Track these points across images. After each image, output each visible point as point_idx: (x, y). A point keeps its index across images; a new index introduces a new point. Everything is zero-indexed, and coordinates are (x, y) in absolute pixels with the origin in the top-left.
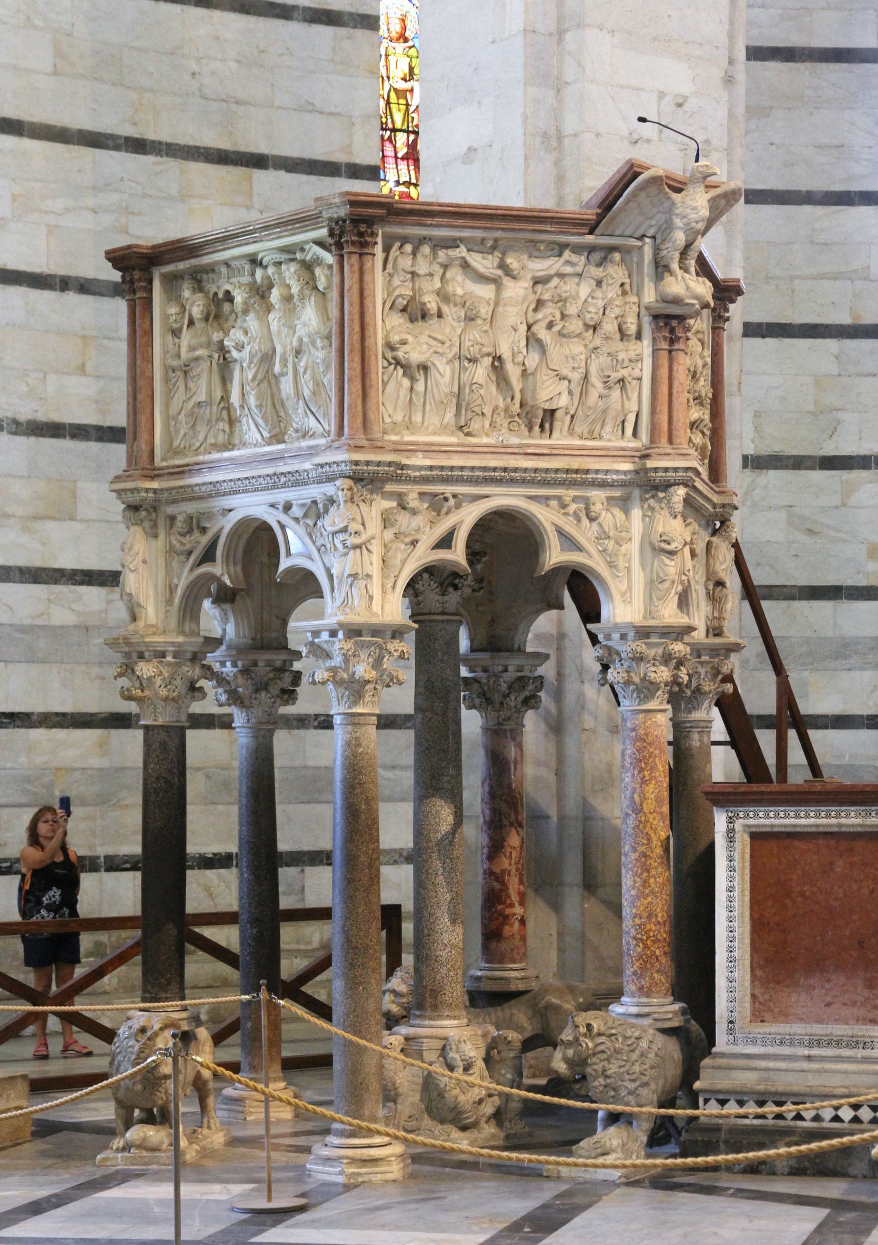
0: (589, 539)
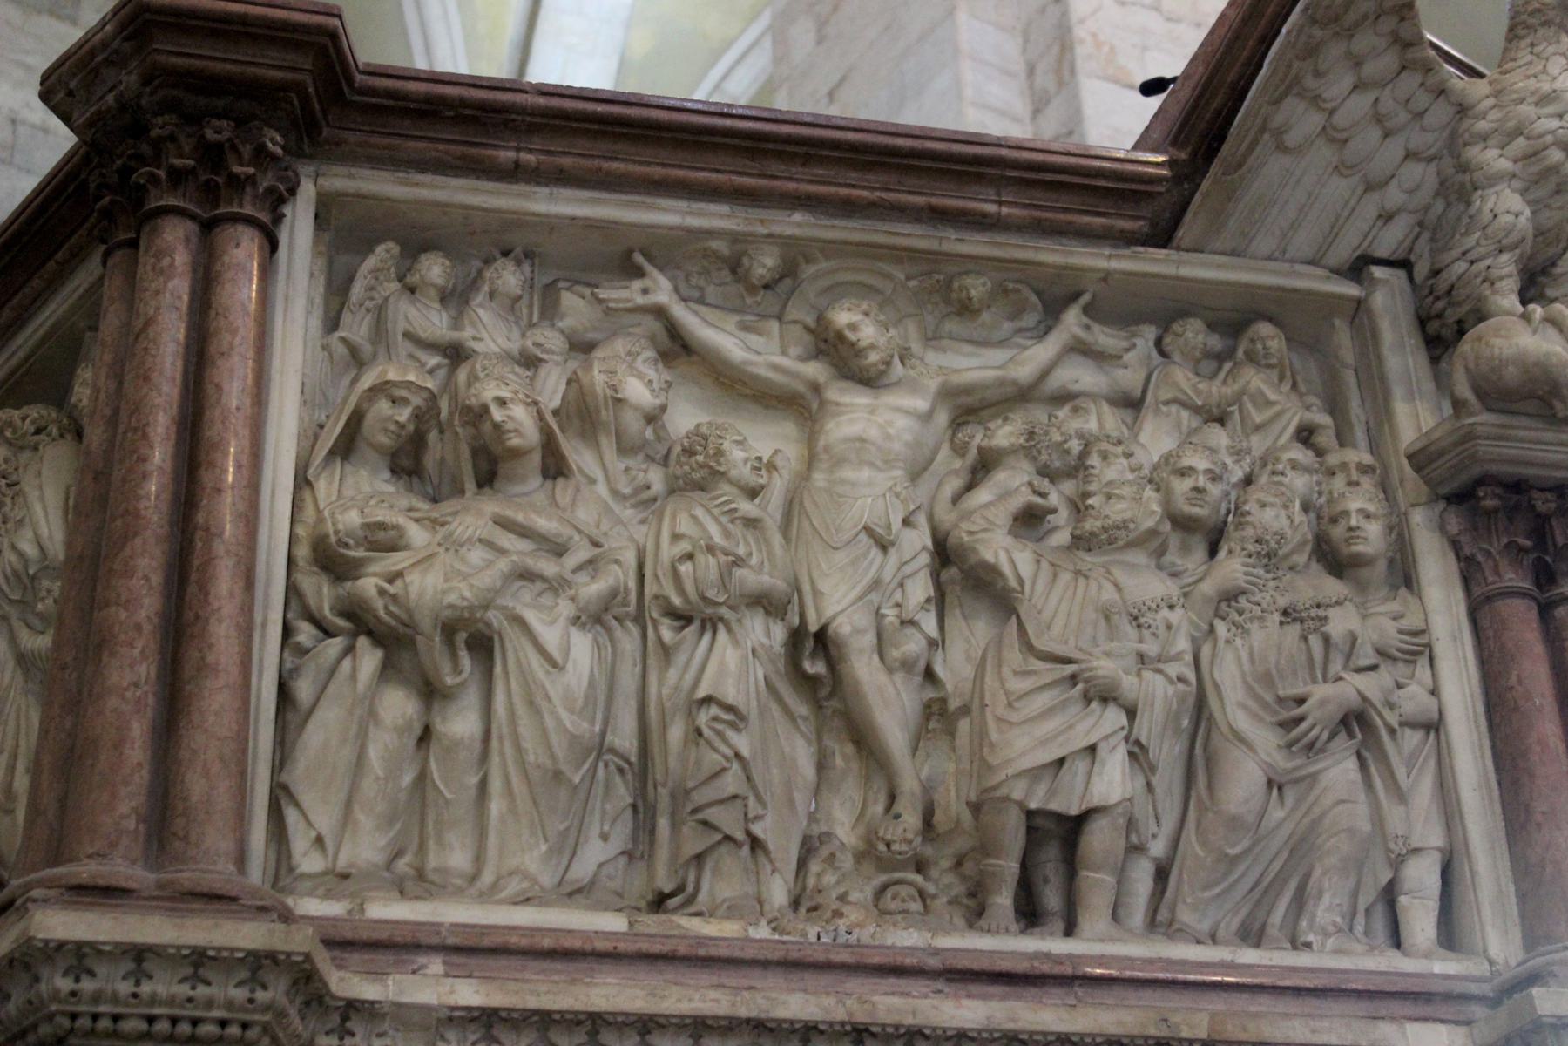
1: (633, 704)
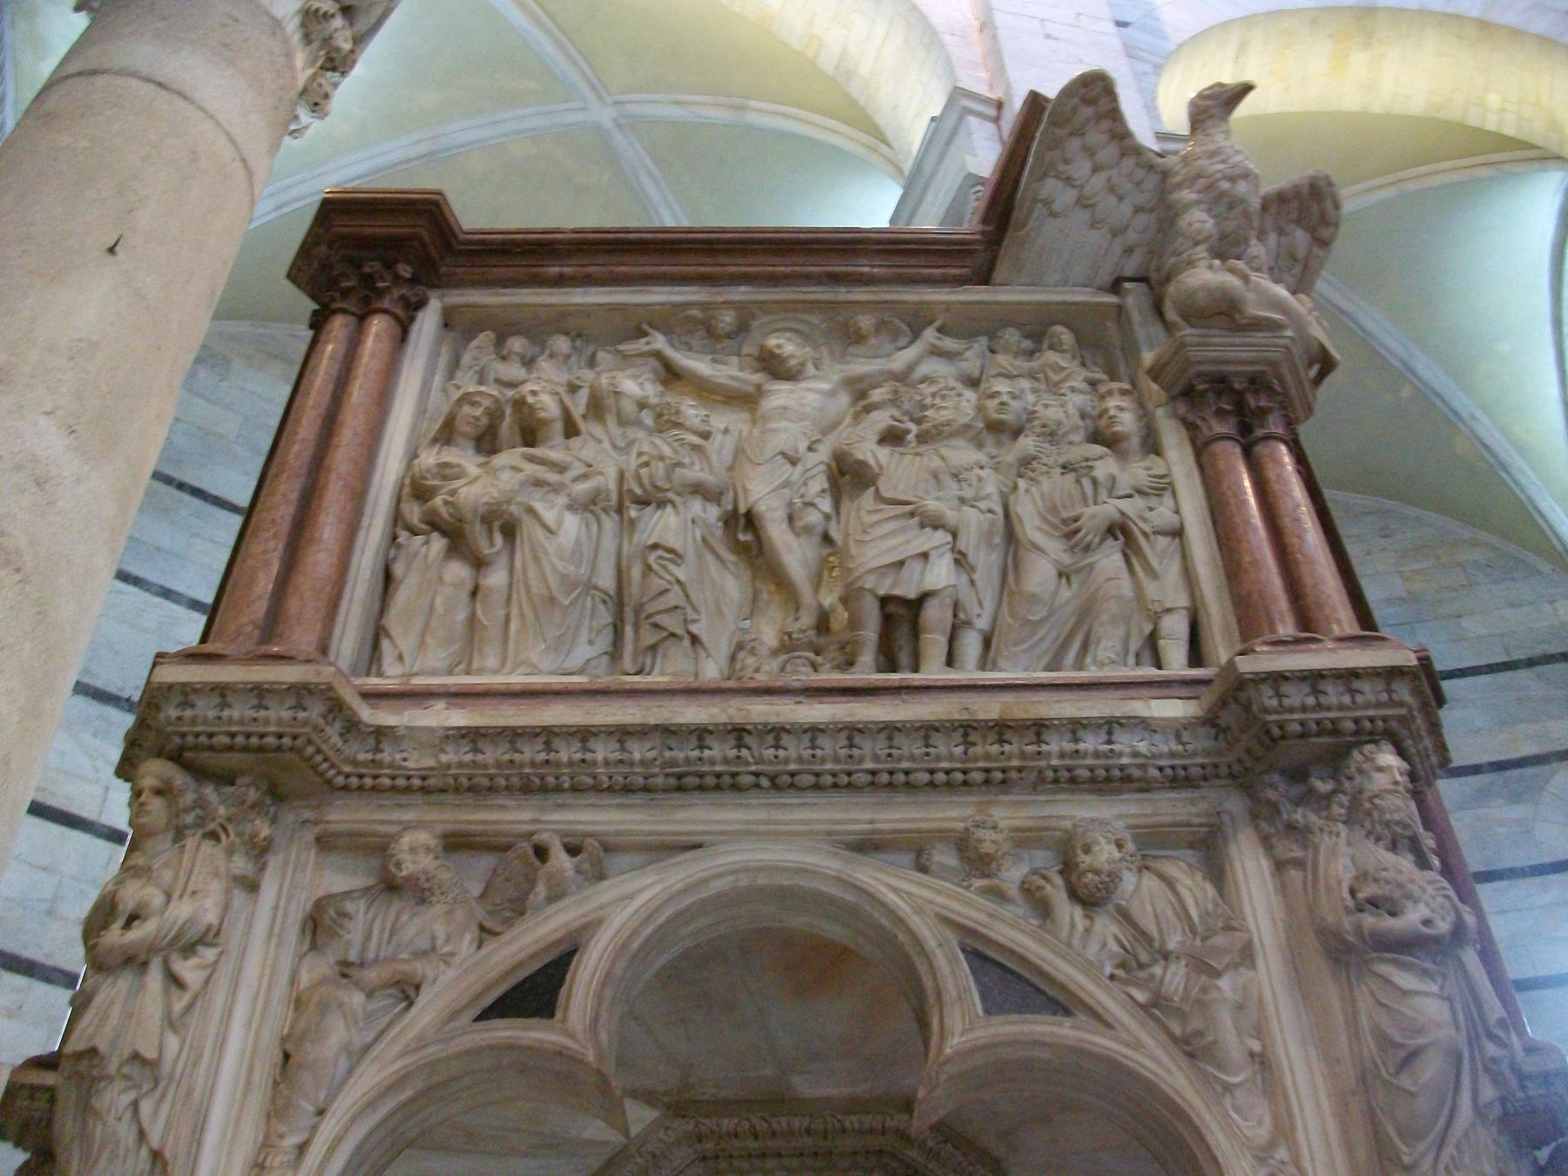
0: (1089, 968)
1: (613, 560)
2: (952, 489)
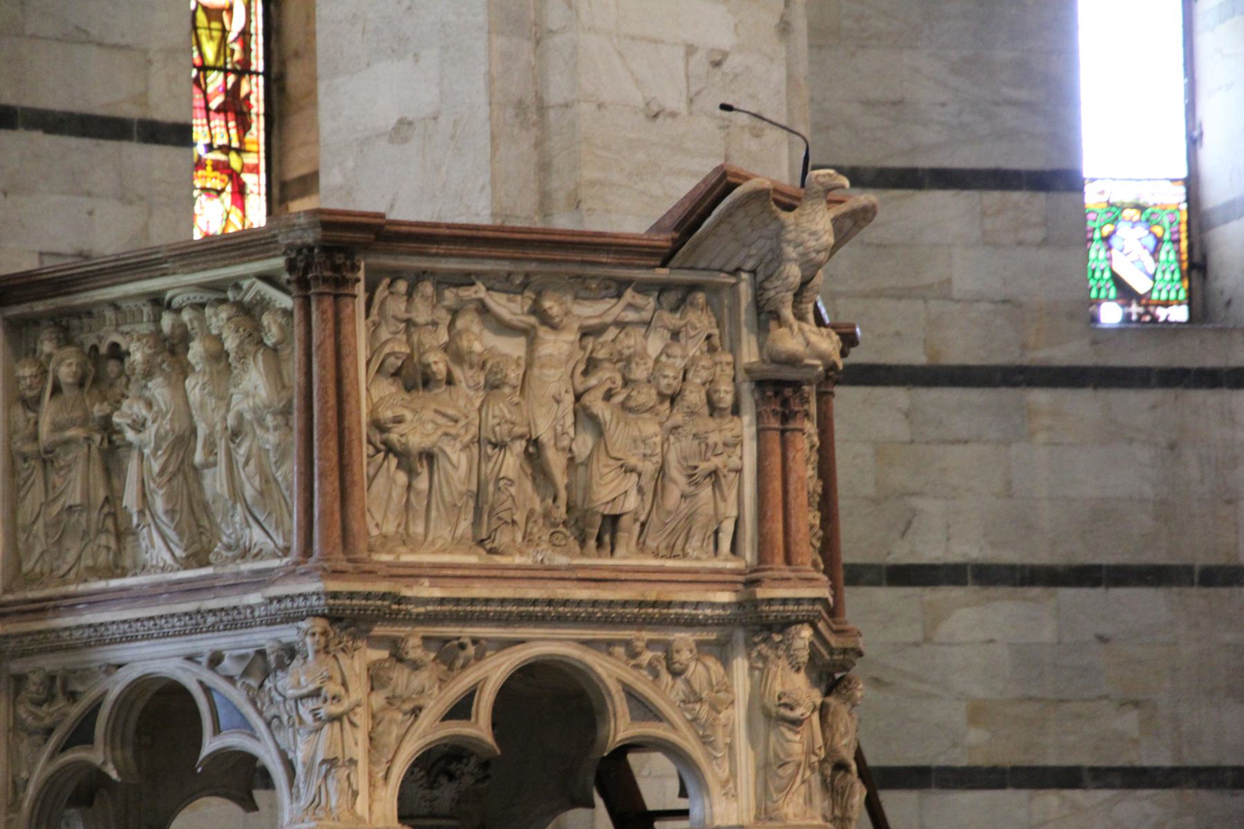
0: (672, 704)
2: (642, 449)
